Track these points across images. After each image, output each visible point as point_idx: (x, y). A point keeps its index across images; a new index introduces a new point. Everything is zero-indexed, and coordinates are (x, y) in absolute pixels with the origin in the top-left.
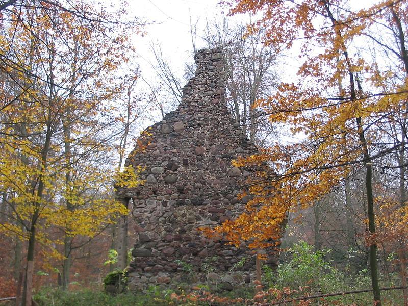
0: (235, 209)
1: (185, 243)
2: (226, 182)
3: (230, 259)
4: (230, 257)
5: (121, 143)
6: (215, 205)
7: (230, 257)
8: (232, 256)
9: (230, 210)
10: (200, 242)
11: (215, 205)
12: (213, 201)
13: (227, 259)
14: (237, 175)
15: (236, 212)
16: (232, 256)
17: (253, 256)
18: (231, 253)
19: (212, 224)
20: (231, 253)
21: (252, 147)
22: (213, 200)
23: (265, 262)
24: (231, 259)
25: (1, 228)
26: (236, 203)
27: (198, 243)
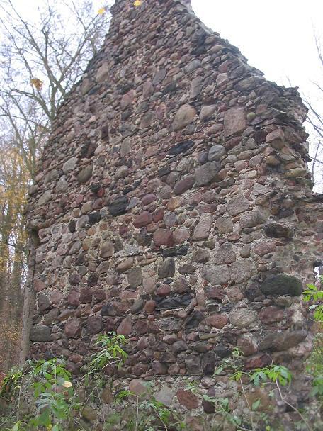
0: (182, 205)
1: (97, 306)
2: (166, 146)
3: (172, 342)
4: (173, 336)
5: (76, 79)
6: (145, 207)
7: (173, 336)
8: (176, 332)
9: (172, 210)
10: (119, 300)
11: (145, 207)
12: (144, 198)
13: (166, 342)
14: (186, 122)
15: (185, 212)
16: (176, 332)
17: (222, 331)
18: (174, 325)
19: (138, 254)
20: (174, 325)
21: (216, 47)
22: (143, 196)
23: (252, 346)
24: (175, 341)
25: (187, 429)
26: (184, 190)
27: (116, 303)
